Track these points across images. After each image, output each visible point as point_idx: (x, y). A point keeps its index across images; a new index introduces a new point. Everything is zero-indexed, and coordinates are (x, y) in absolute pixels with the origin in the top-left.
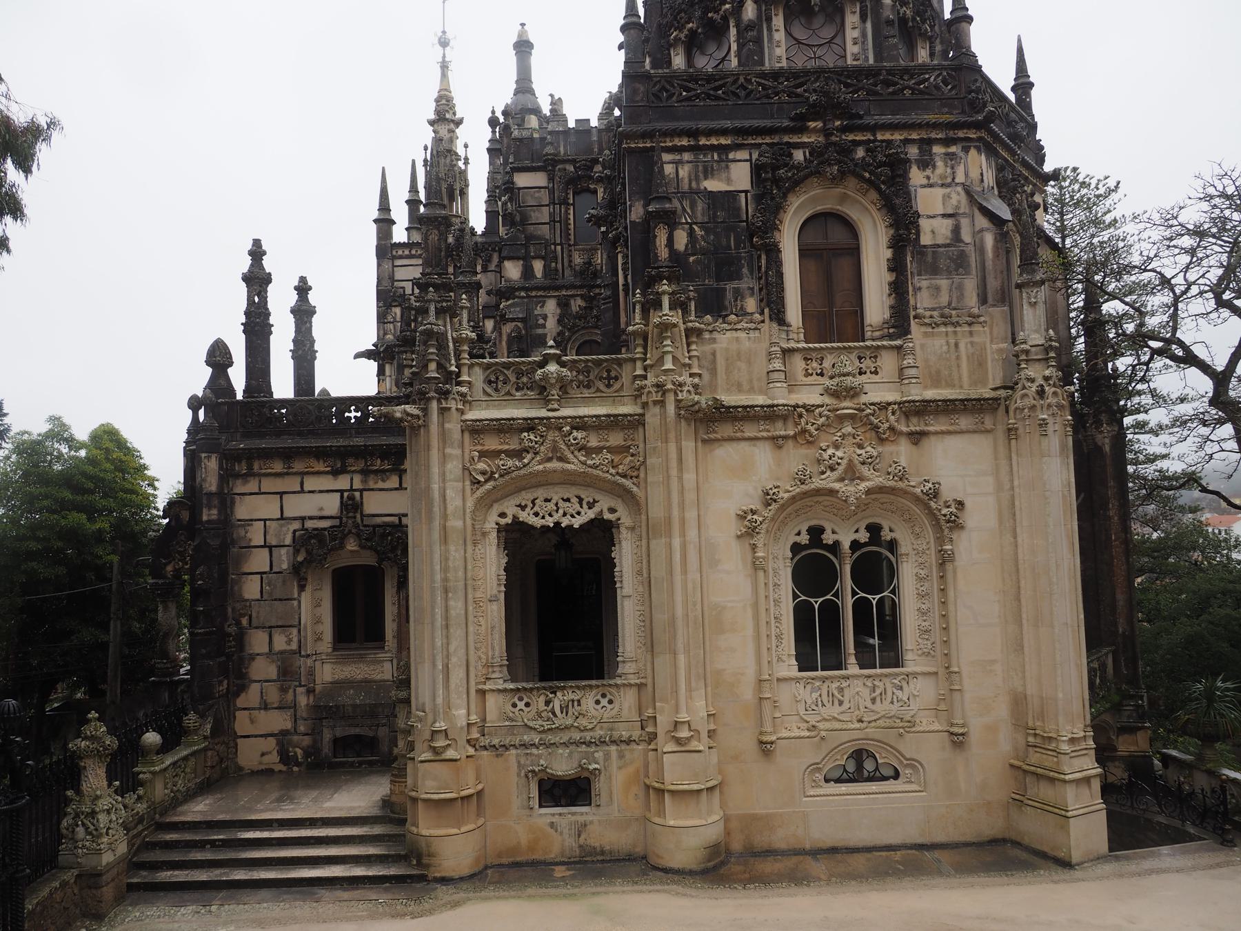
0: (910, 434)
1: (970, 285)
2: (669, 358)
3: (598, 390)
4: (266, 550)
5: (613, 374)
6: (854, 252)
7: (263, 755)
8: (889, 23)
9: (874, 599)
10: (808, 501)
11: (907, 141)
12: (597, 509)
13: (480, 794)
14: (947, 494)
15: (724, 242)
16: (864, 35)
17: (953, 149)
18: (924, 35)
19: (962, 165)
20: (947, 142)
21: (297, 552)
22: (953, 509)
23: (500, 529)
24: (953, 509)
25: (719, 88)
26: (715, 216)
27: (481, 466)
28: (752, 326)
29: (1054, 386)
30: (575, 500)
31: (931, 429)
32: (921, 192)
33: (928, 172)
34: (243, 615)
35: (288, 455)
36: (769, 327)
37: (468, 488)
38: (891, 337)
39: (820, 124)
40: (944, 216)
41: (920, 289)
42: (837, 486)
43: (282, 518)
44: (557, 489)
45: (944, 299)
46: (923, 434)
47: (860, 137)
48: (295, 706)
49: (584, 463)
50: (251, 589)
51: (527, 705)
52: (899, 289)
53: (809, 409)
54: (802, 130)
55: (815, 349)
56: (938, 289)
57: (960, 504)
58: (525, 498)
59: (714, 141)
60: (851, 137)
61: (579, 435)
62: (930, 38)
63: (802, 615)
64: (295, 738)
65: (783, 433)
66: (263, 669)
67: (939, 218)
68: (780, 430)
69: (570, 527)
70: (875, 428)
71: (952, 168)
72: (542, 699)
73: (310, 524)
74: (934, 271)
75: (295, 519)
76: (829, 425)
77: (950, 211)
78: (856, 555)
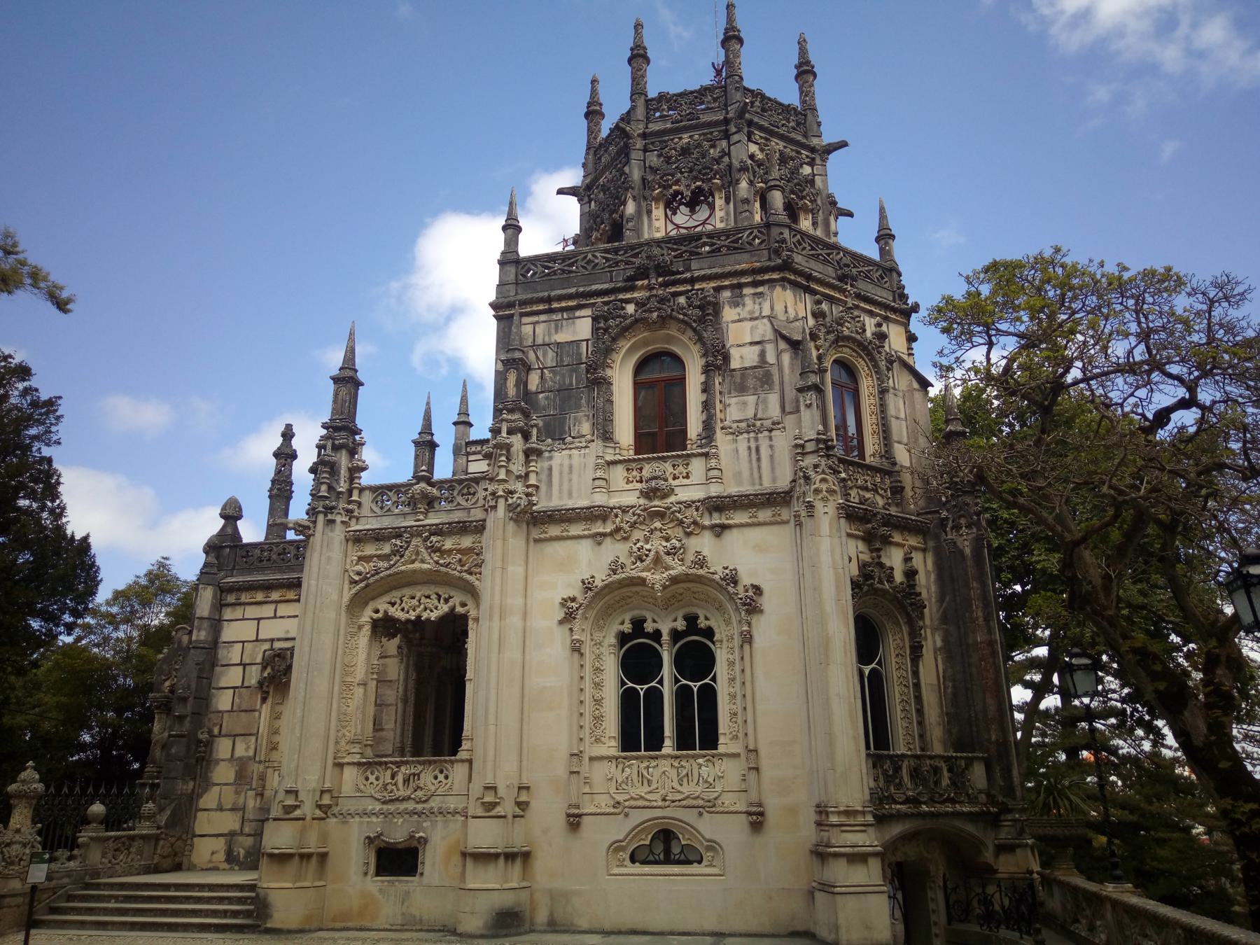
0: (713, 527)
1: (773, 399)
2: (503, 471)
3: (459, 504)
4: (241, 668)
5: (472, 491)
6: (682, 381)
7: (213, 853)
8: (746, 201)
9: (695, 686)
10: (625, 591)
11: (718, 289)
12: (450, 604)
13: (323, 857)
14: (746, 580)
15: (567, 381)
16: (728, 214)
17: (760, 289)
18: (806, 210)
20: (755, 284)
21: (264, 668)
22: (750, 593)
23: (375, 624)
24: (750, 593)
25: (571, 265)
26: (562, 361)
27: (359, 568)
29: (823, 472)
30: (434, 596)
31: (731, 522)
33: (738, 310)
34: (215, 725)
35: (268, 587)
36: (597, 447)
37: (346, 586)
38: (701, 446)
39: (646, 282)
40: (751, 344)
42: (644, 574)
43: (257, 640)
44: (419, 587)
45: (750, 413)
46: (724, 527)
47: (682, 289)
48: (244, 809)
49: (437, 562)
50: (224, 701)
51: (377, 779)
52: (707, 406)
53: (625, 510)
54: (633, 289)
56: (745, 403)
57: (758, 590)
58: (396, 595)
59: (563, 304)
60: (673, 289)
61: (434, 539)
62: (812, 211)
63: (628, 701)
64: (241, 839)
65: (601, 530)
66: (223, 773)
68: (599, 528)
69: (428, 620)
70: (681, 523)
72: (389, 773)
73: (277, 645)
74: (742, 389)
75: (266, 640)
76: (641, 523)
78: (677, 646)
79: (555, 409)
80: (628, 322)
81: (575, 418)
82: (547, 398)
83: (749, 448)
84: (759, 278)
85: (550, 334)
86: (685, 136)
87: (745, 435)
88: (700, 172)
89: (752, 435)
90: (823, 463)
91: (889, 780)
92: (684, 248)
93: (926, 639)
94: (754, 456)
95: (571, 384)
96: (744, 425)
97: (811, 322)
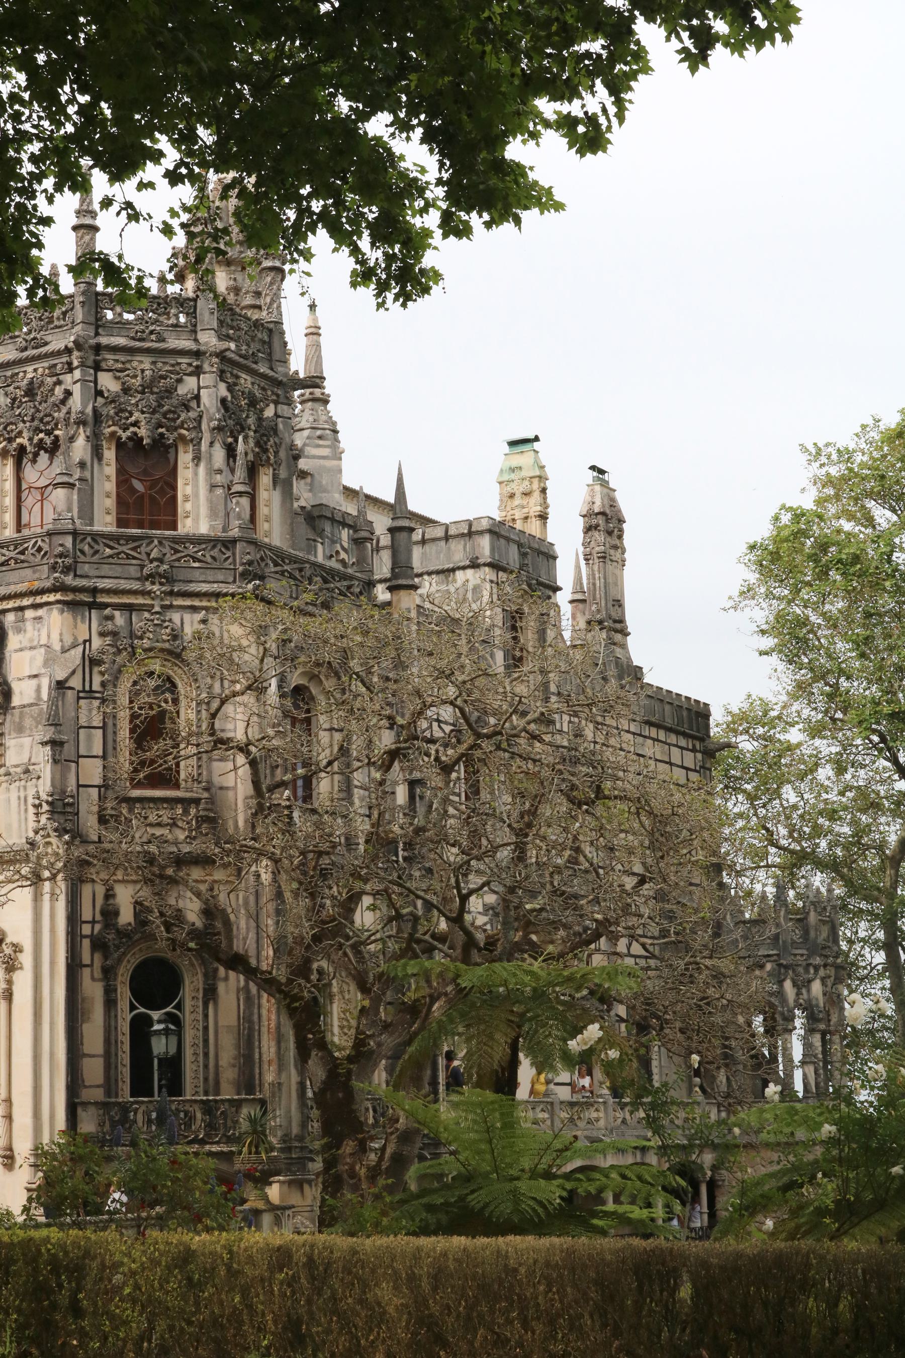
17: (40, 612)
20: (36, 606)
32: (15, 656)
33: (20, 637)
40: (30, 677)
56: (22, 746)
74: (20, 729)
83: (19, 798)
84: (39, 600)
86: (30, 369)
88: (41, 420)
89: (23, 782)
90: (49, 826)
91: (114, 1124)
93: (226, 979)
94: (23, 807)
96: (19, 770)
97: (97, 642)
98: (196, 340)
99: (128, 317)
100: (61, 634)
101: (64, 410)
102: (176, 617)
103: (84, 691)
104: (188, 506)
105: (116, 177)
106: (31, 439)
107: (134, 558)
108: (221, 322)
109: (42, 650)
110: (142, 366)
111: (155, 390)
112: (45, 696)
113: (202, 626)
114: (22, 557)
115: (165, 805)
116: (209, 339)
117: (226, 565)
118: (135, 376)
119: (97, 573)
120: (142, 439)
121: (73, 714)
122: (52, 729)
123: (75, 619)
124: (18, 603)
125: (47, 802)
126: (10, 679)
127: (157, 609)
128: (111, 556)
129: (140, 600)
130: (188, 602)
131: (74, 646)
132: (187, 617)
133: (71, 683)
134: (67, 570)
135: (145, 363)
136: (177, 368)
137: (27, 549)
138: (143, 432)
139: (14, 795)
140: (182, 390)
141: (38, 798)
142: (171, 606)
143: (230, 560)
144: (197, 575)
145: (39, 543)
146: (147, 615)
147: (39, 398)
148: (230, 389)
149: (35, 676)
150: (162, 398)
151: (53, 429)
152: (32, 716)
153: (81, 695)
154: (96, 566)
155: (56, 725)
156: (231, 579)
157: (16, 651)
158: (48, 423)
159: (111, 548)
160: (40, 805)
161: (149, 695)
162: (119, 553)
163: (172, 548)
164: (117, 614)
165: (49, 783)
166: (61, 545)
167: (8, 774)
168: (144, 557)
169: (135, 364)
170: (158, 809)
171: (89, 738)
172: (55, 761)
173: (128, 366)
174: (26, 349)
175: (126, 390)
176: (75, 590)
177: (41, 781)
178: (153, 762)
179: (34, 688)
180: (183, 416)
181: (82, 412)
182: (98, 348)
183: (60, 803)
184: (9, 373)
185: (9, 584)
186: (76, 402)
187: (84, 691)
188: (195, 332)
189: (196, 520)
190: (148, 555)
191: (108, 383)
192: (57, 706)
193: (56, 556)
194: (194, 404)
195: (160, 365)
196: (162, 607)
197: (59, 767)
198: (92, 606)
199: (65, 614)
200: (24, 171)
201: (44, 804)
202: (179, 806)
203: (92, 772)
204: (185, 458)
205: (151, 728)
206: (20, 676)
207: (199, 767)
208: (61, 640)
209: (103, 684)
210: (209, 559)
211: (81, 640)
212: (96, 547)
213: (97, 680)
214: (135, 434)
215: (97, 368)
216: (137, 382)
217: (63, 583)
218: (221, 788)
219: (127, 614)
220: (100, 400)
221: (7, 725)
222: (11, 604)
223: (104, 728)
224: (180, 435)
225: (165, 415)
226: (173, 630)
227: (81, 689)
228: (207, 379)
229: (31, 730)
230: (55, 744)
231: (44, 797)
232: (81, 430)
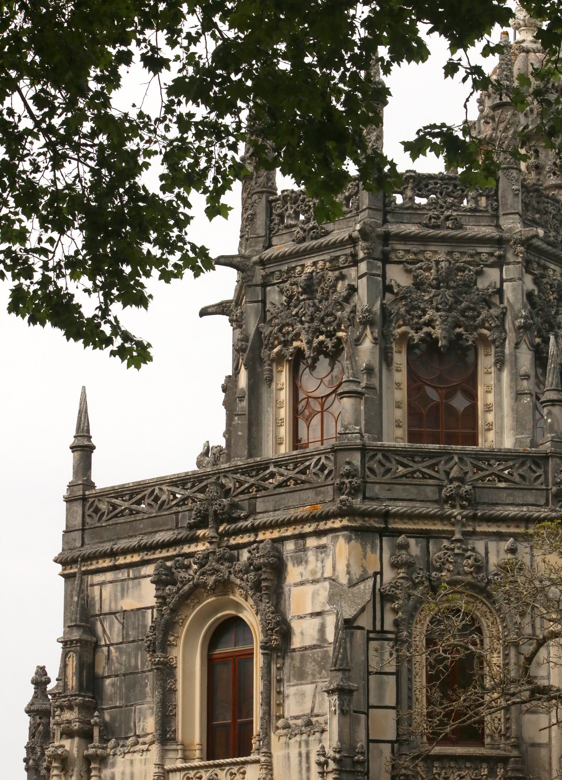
15: (133, 663)
17: (324, 540)
19: (331, 557)
20: (318, 534)
25: (139, 503)
26: (128, 635)
28: (145, 747)
32: (295, 591)
33: (301, 569)
41: (288, 696)
54: (195, 540)
55: (236, 764)
56: (303, 695)
59: (129, 559)
67: (308, 618)
71: (322, 562)
74: (301, 676)
77: (318, 610)
79: (121, 699)
80: (186, 588)
81: (140, 711)
82: (113, 685)
83: (300, 754)
84: (322, 526)
85: (116, 600)
86: (309, 262)
87: (298, 738)
88: (322, 320)
89: (304, 737)
92: (252, 480)
95: (136, 666)
96: (299, 722)
97: (389, 575)
98: (498, 226)
99: (421, 201)
100: (348, 566)
101: (348, 309)
102: (480, 546)
103: (374, 631)
104: (491, 417)
105: (459, 42)
106: (309, 342)
107: (431, 477)
108: (526, 205)
109: (327, 584)
110: (437, 257)
111: (452, 284)
112: (330, 636)
113: (510, 556)
114: (303, 477)
115: (468, 765)
116: (512, 225)
117: (537, 484)
118: (429, 269)
119: (389, 495)
120: (437, 340)
121: (363, 658)
122: (340, 674)
123: (364, 548)
124: (298, 530)
125: (334, 759)
126: (289, 617)
127: (458, 536)
128: (404, 476)
129: (439, 527)
130: (493, 529)
131: (363, 579)
132: (492, 545)
133: (361, 622)
134: (355, 491)
135: (440, 255)
136: (477, 259)
137: (308, 467)
138: (438, 332)
139: (294, 752)
140: (482, 284)
141: (324, 755)
142: (474, 533)
143: (542, 479)
144: (504, 496)
145: (323, 460)
146: (446, 543)
147: (319, 295)
148: (536, 281)
149: (319, 614)
150: (460, 293)
151: (335, 331)
152: (314, 660)
153: (372, 635)
154: (387, 487)
155: (344, 670)
156: (543, 502)
157: (296, 585)
158: (330, 323)
159: (405, 466)
160: (326, 763)
161: (454, 636)
162: (414, 472)
163: (474, 466)
164: (412, 541)
165: (336, 737)
166: (348, 463)
167: (287, 726)
168: (442, 476)
169: (428, 255)
170: (460, 769)
171: (381, 686)
172: (343, 712)
173: (421, 257)
174: (303, 240)
175: (419, 285)
176: (364, 514)
177: (326, 735)
178: (459, 714)
179: (317, 627)
180: (484, 314)
181: (369, 311)
182: (387, 238)
183: (348, 761)
184: (285, 268)
185: (288, 508)
186: (362, 298)
187: (374, 631)
188: (497, 217)
189: (500, 434)
190: (447, 473)
191: (398, 276)
192: (345, 649)
193: (342, 476)
194: (496, 300)
195: (457, 255)
196: (464, 534)
197: (347, 719)
198: (384, 533)
199: (353, 542)
200: (356, 38)
201: (331, 762)
202: (484, 765)
203: (385, 724)
204: (486, 361)
205: (456, 675)
206: (301, 614)
207: (507, 720)
208: (348, 573)
209: (396, 623)
210: (517, 479)
211: (371, 572)
212: (388, 465)
213: (389, 618)
214: (429, 334)
215: (386, 260)
216: (432, 275)
217: (351, 507)
218: (533, 745)
219: (424, 541)
220: (389, 296)
221: (286, 670)
222: (290, 532)
223: (397, 674)
224: (482, 336)
225: (463, 313)
226: (476, 560)
227: (370, 628)
228: (509, 271)
229: (314, 676)
230: (343, 692)
231: (330, 752)
232: (368, 331)
